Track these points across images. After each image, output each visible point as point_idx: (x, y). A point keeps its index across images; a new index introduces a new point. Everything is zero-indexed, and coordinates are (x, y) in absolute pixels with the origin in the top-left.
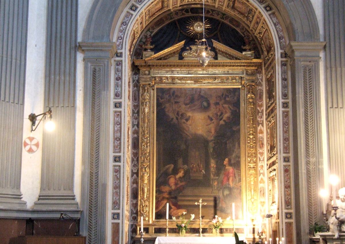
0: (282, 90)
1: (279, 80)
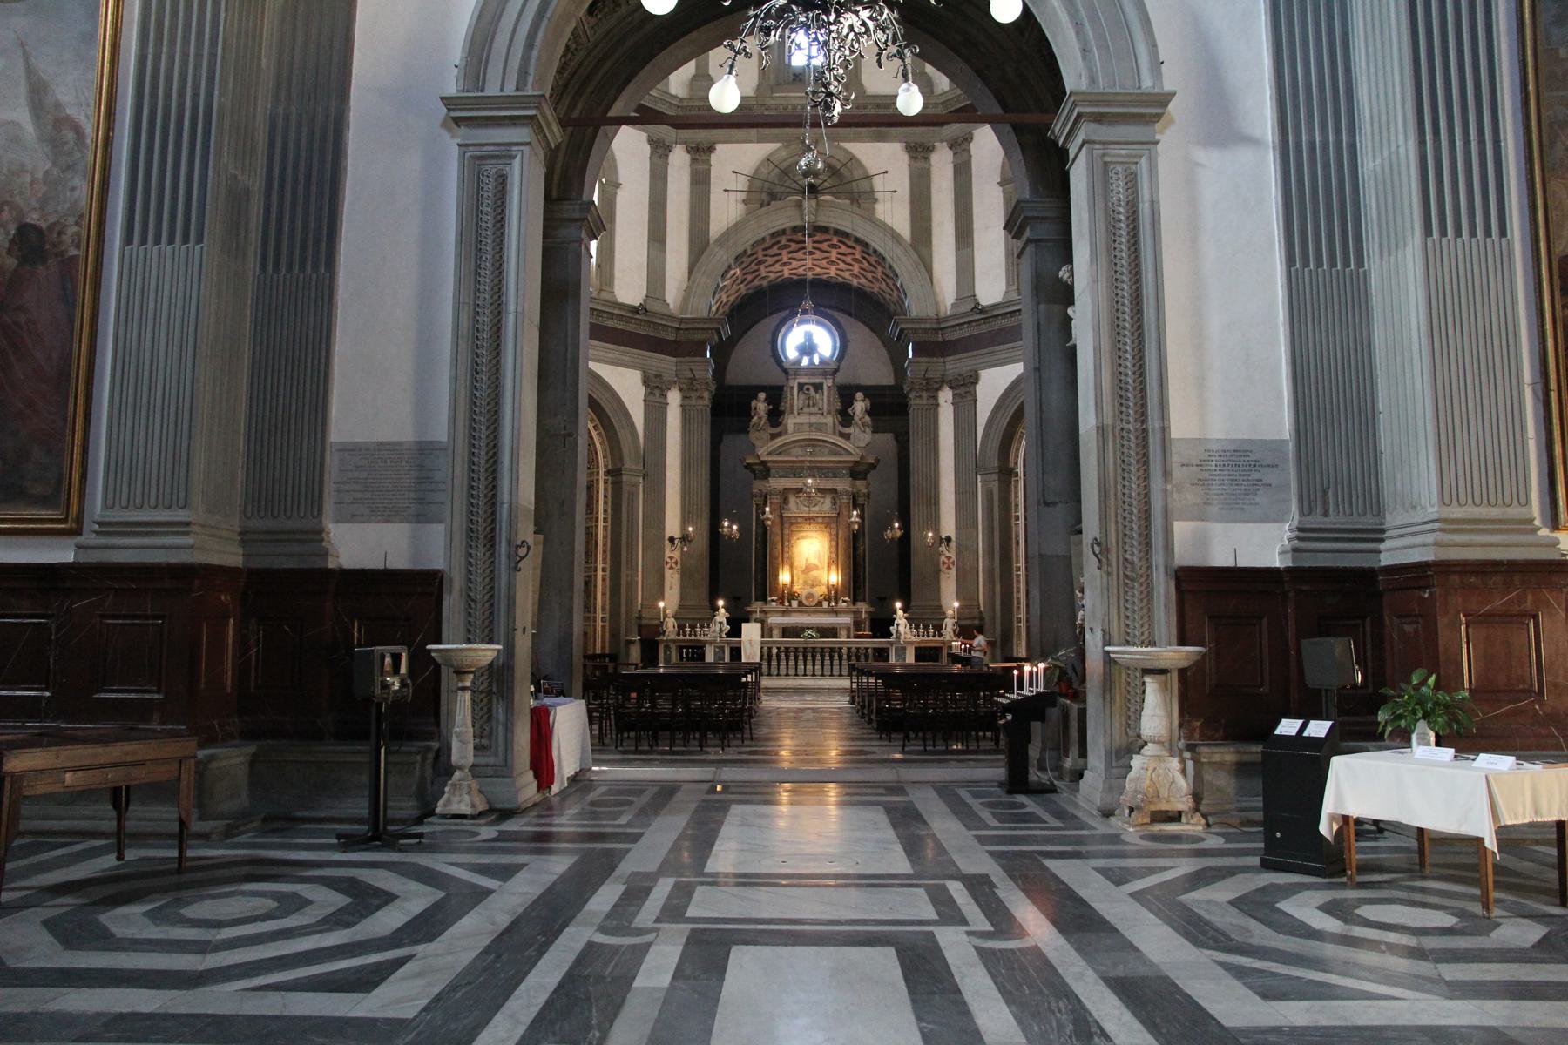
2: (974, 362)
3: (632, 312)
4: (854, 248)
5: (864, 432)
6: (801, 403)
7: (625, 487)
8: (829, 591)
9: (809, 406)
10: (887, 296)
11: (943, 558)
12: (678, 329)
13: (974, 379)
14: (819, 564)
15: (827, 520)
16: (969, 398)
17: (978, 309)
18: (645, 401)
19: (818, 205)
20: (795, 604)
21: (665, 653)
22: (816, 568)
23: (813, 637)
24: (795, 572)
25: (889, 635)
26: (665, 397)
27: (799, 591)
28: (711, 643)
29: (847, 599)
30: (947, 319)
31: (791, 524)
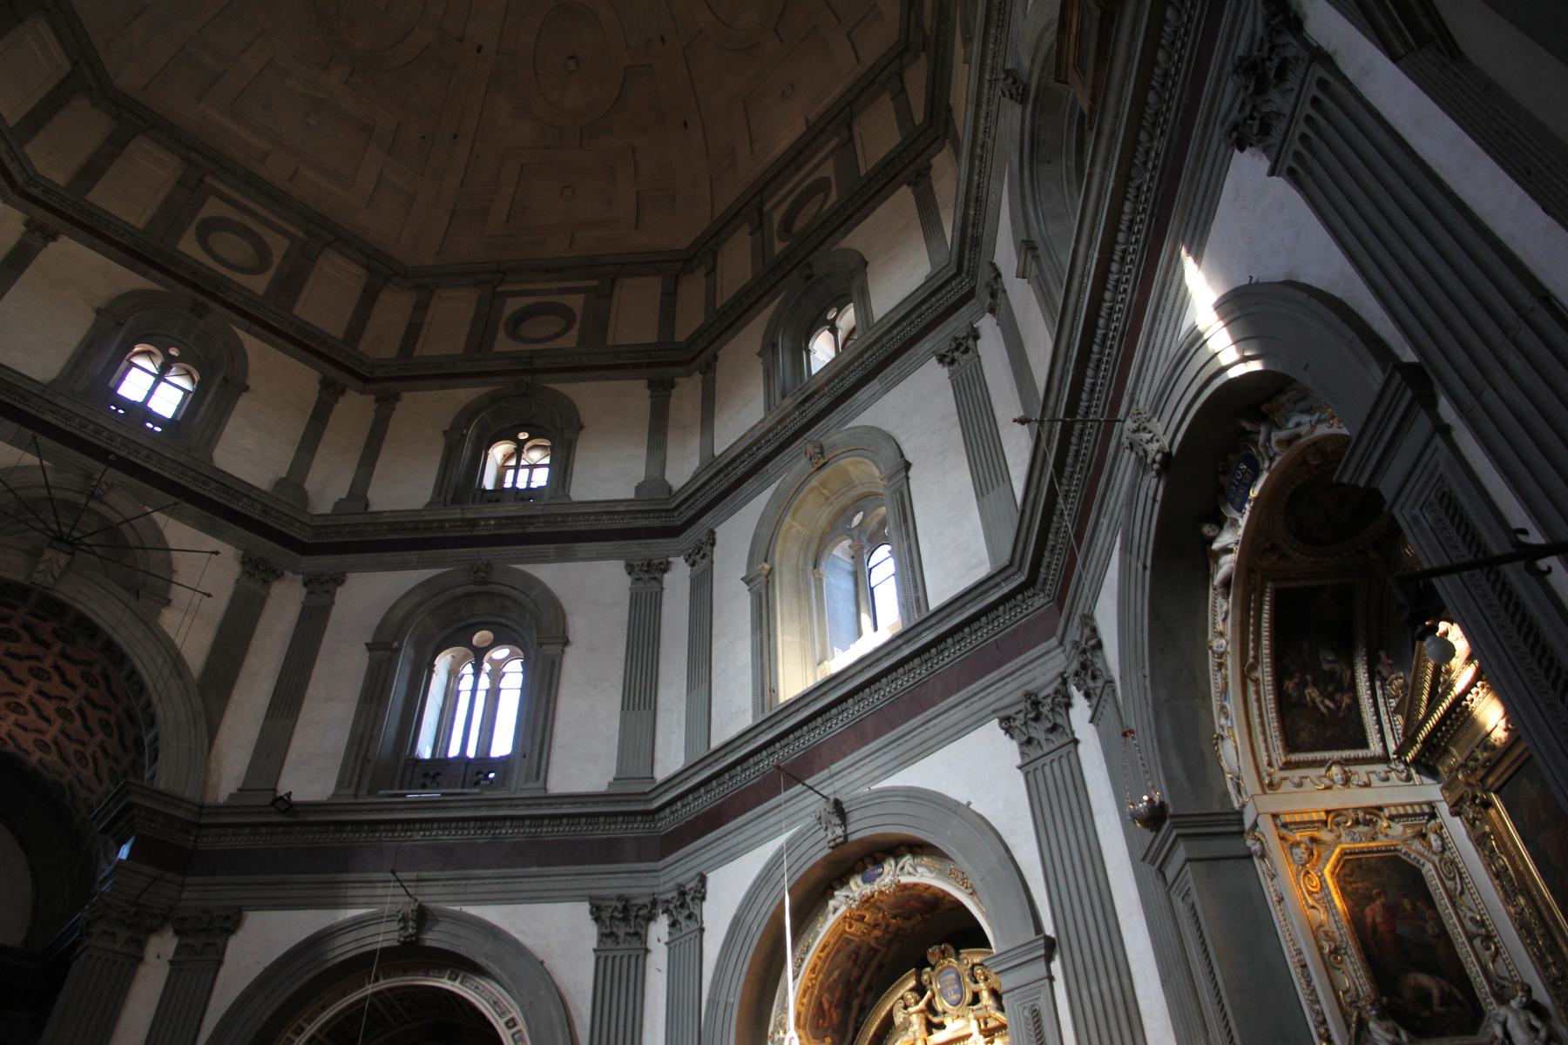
13: (231, 923)
17: (285, 805)
19: (69, 566)
30: (219, 809)
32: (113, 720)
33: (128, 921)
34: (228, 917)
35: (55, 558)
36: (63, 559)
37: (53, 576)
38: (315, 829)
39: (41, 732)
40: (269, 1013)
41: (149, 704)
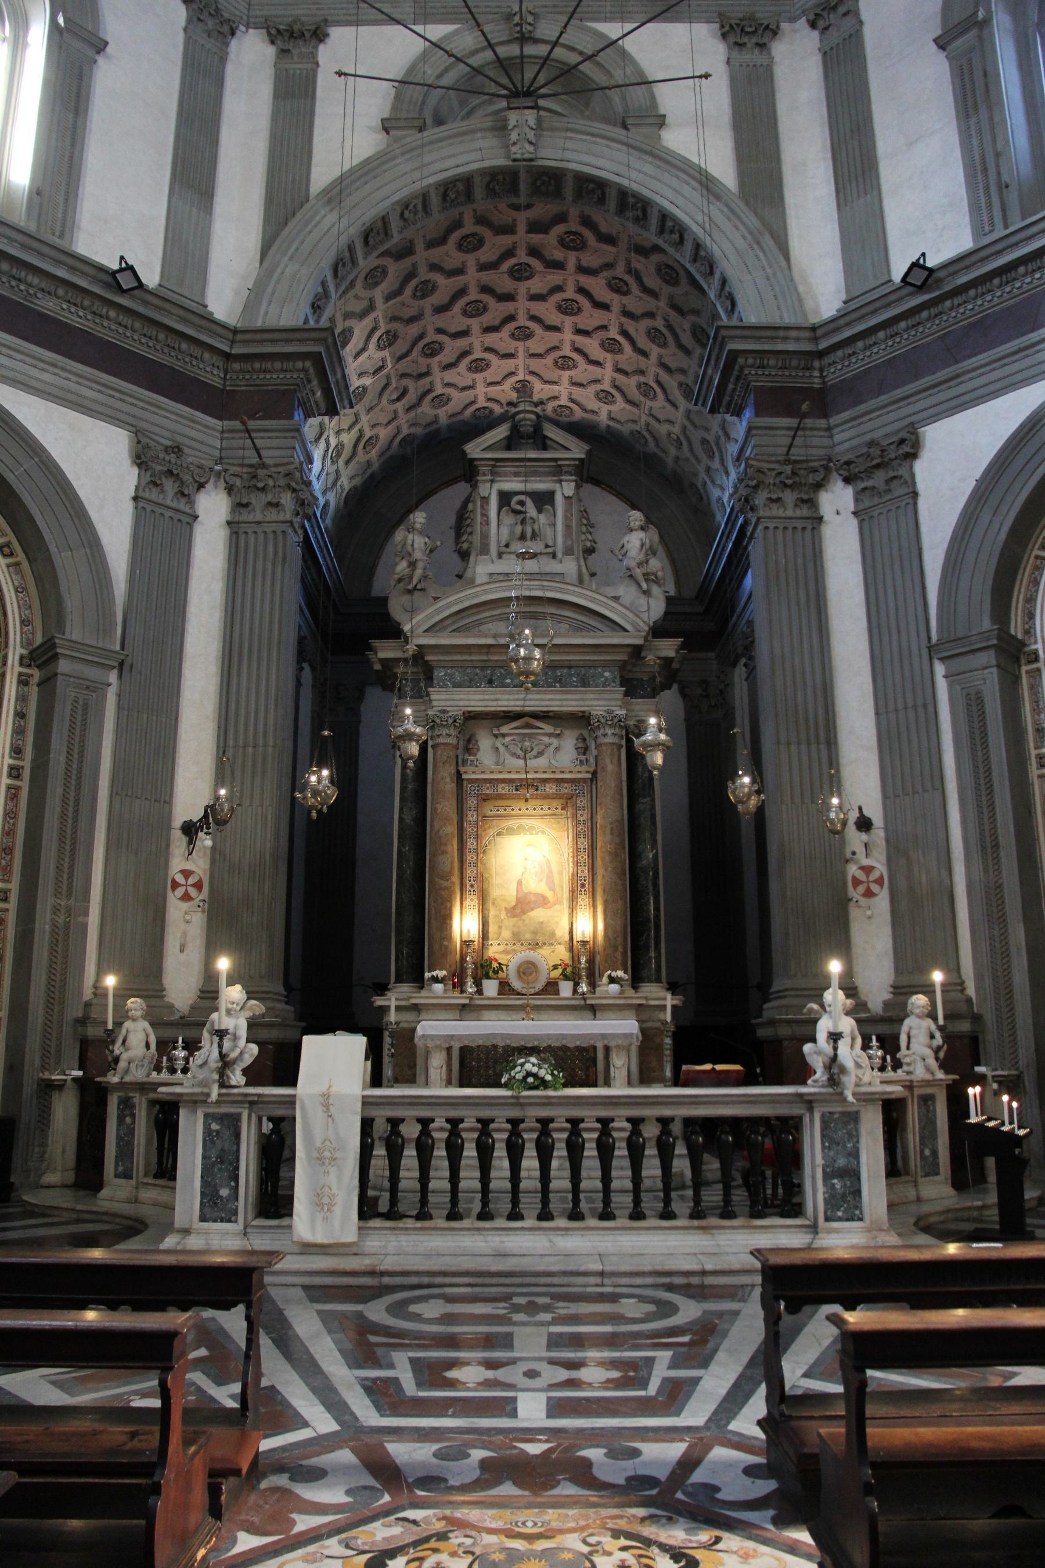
0: (12, 737)
1: (8, 712)
2: (911, 409)
3: (106, 285)
4: (605, 307)
5: (647, 593)
6: (505, 532)
7: (66, 693)
8: (575, 957)
9: (523, 537)
10: (663, 429)
11: (853, 870)
12: (228, 357)
14: (549, 894)
15: (566, 789)
16: (899, 490)
18: (135, 499)
20: (491, 987)
21: (121, 1120)
22: (543, 901)
23: (543, 1084)
24: (492, 913)
25: (802, 1072)
26: (191, 502)
27: (503, 959)
28: (197, 1101)
29: (620, 973)
31: (486, 799)
32: (659, 323)
33: (789, 482)
34: (902, 441)
35: (520, 120)
36: (531, 117)
37: (531, 143)
38: (972, 293)
39: (596, 381)
40: (1006, 529)
41: (698, 246)
